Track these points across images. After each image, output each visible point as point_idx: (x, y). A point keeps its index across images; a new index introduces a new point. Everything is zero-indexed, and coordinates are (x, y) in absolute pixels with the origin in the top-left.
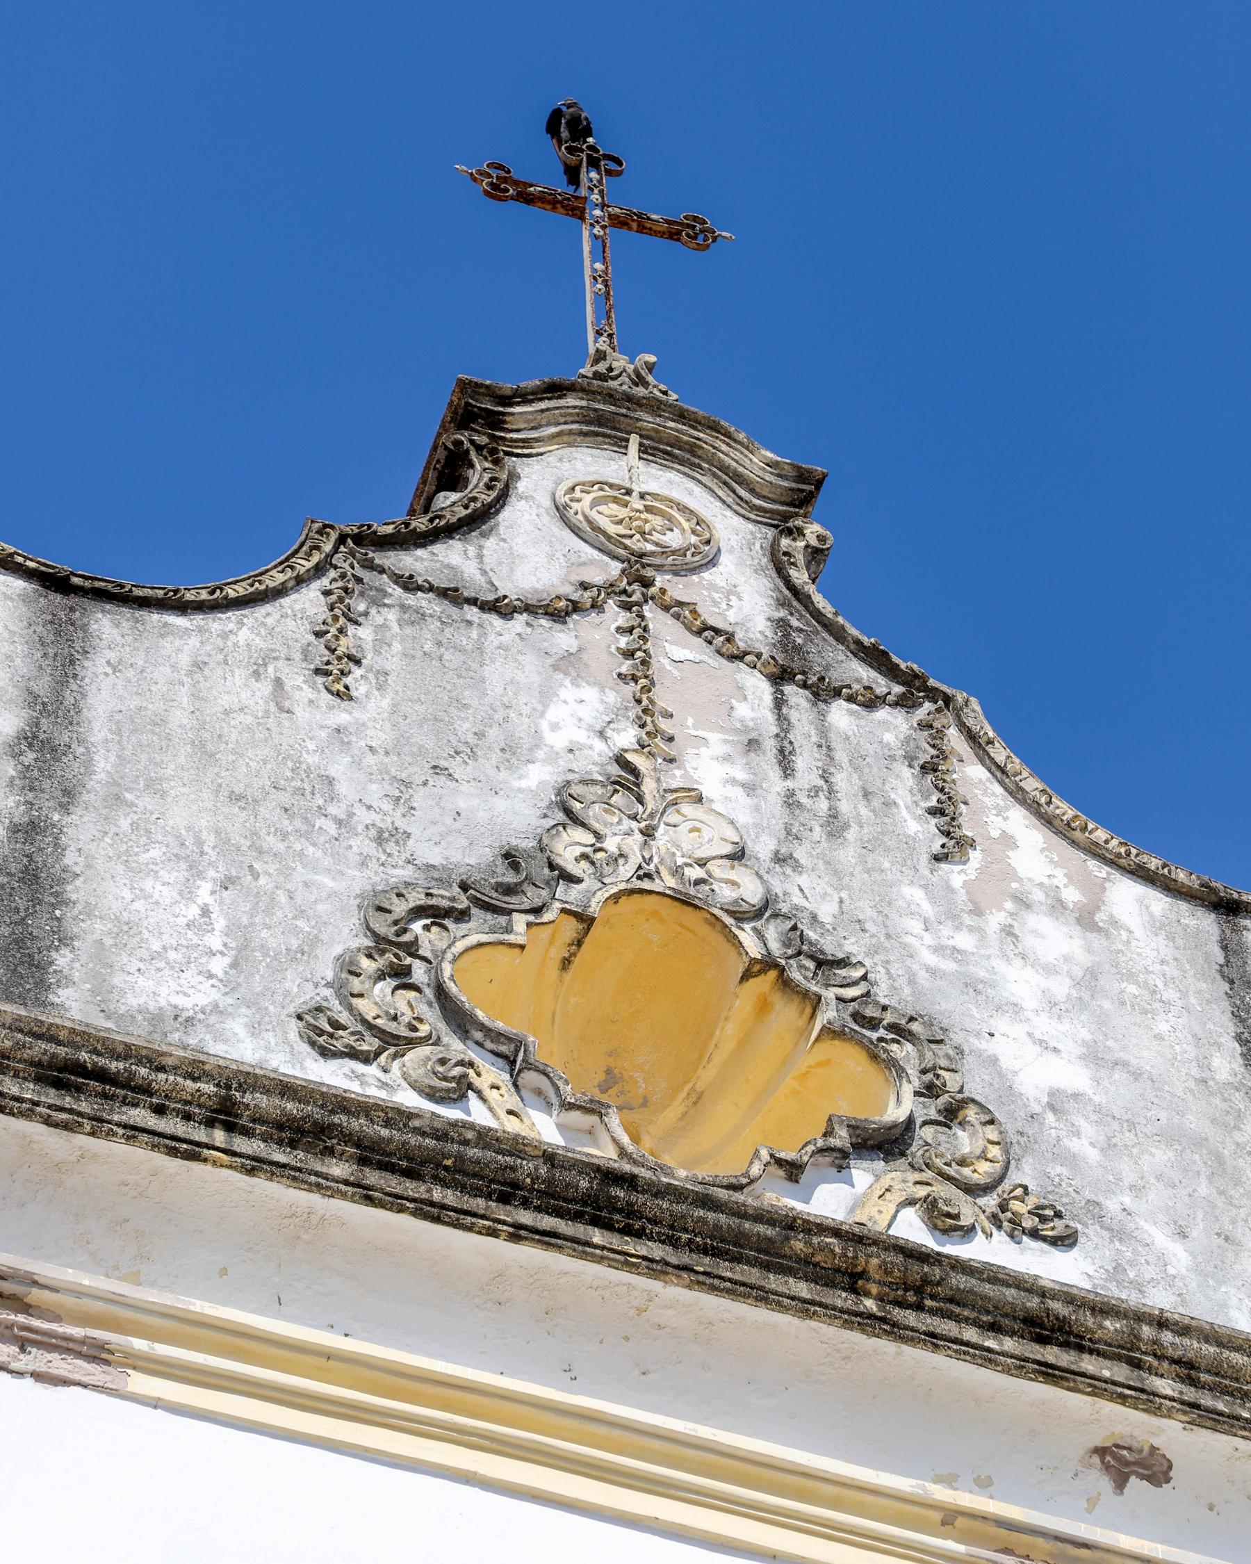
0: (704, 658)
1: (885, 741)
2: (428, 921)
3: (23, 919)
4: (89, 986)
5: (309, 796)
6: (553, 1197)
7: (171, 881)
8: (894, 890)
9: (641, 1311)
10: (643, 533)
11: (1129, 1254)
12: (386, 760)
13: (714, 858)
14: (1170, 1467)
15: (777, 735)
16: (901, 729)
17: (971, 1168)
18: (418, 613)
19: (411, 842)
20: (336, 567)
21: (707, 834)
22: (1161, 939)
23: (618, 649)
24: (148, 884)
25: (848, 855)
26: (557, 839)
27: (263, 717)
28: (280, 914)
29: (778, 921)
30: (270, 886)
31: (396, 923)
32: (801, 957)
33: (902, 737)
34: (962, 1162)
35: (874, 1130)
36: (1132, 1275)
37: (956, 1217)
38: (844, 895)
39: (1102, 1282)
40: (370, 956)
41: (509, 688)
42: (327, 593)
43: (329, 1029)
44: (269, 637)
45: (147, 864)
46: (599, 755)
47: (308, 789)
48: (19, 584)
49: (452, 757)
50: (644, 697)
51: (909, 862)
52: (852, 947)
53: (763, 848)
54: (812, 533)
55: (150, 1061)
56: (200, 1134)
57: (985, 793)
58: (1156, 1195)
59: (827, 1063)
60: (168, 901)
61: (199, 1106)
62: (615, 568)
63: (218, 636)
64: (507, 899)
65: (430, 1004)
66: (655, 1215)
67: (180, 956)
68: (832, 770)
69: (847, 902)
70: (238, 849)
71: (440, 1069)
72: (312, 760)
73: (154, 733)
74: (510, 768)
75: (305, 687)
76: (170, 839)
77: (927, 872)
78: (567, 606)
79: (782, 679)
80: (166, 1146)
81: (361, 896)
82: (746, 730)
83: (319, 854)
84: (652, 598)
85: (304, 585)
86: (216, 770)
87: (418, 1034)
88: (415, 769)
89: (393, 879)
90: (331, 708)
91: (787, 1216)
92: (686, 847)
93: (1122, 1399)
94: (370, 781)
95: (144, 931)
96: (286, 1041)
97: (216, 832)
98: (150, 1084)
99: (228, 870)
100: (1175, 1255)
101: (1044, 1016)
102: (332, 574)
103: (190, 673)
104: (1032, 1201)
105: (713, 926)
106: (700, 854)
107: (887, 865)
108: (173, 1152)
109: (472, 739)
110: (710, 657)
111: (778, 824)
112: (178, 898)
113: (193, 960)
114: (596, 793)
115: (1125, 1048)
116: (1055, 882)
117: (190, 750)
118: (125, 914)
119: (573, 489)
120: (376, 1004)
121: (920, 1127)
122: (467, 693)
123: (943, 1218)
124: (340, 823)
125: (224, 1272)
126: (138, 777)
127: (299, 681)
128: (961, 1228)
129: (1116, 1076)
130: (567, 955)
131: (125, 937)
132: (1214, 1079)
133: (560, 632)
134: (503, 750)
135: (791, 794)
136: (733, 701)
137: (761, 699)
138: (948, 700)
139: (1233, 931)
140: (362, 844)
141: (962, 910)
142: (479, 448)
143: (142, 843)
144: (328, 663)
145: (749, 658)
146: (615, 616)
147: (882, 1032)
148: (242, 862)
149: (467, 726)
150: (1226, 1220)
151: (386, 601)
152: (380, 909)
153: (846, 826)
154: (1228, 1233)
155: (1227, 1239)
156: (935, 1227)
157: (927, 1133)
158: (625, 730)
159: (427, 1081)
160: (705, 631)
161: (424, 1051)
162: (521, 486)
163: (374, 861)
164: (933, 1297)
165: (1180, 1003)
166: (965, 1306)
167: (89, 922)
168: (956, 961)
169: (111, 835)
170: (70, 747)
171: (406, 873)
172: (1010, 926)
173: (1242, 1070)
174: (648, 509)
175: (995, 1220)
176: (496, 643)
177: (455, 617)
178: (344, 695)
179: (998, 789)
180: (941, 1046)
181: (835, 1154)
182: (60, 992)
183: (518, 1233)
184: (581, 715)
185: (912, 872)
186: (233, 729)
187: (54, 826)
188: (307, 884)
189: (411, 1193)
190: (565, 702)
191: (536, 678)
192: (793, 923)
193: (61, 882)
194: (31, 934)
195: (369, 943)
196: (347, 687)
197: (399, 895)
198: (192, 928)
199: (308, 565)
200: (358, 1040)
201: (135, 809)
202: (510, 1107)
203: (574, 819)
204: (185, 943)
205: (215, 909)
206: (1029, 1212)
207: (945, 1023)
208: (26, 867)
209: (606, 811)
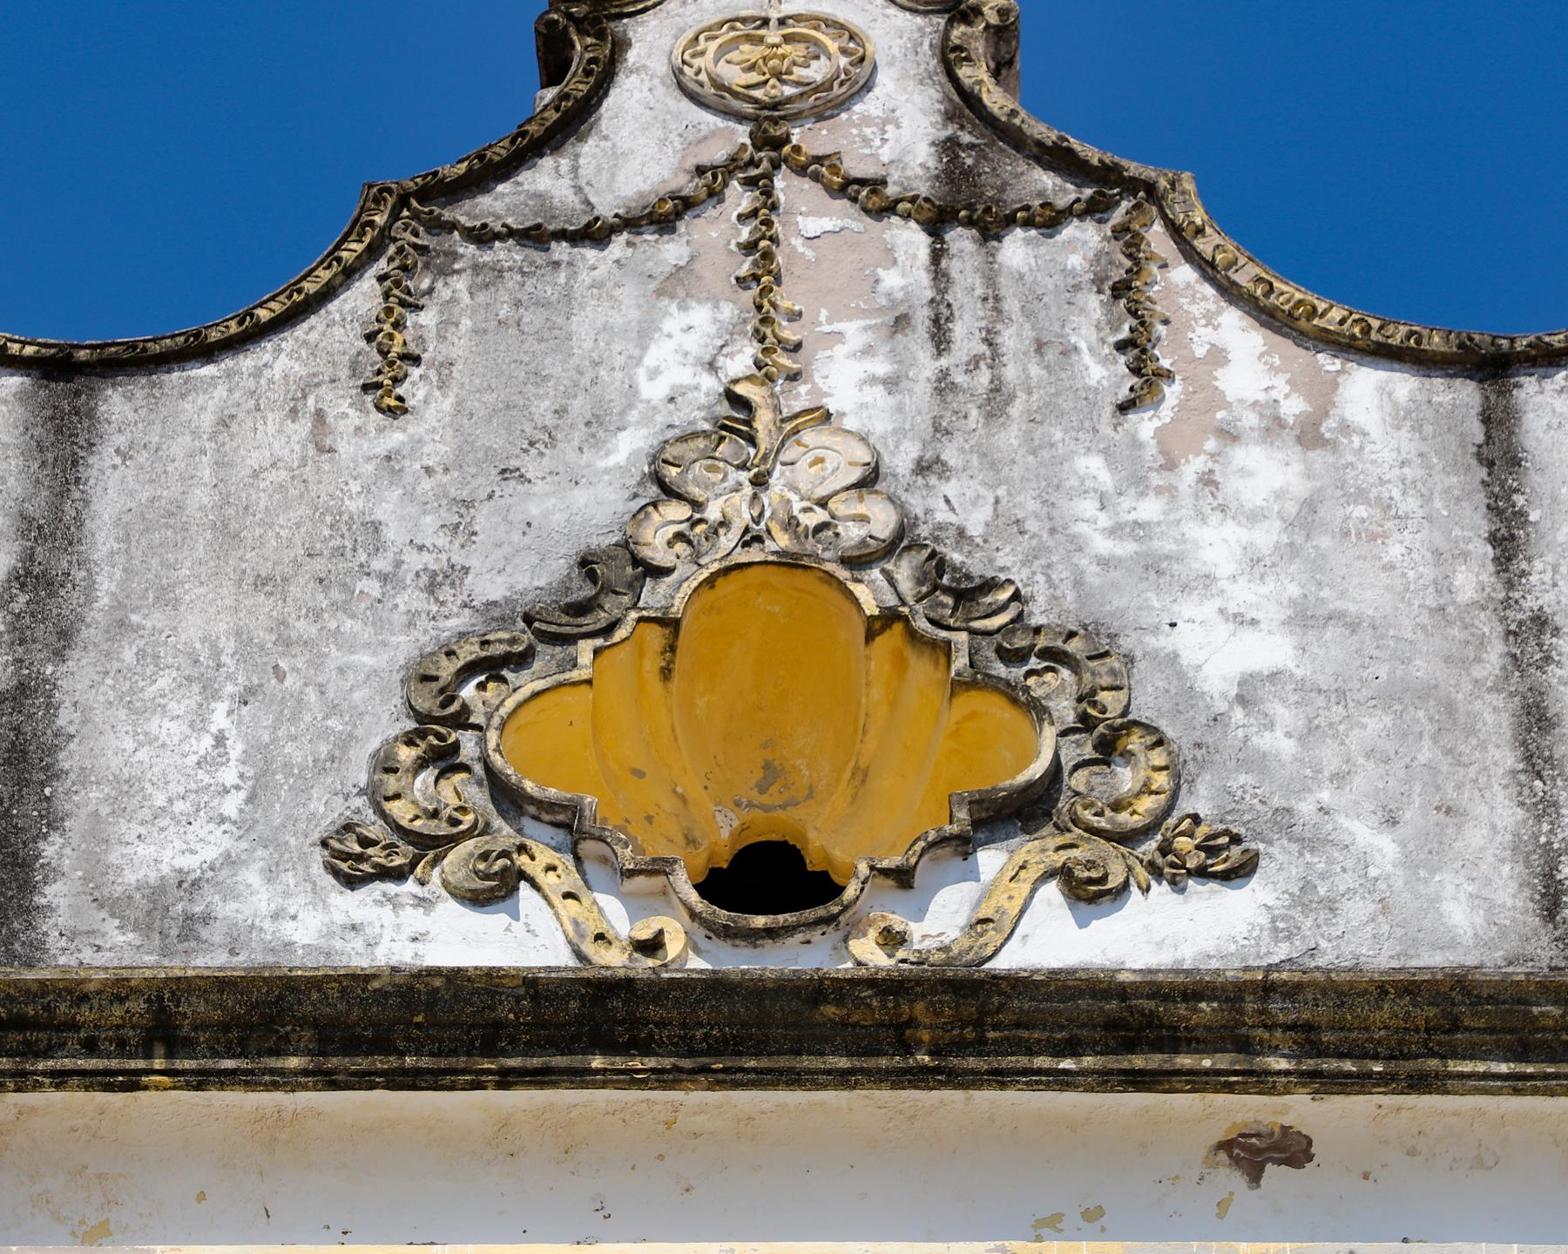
0: (848, 222)
1: (1069, 267)
2: (482, 678)
3: (7, 810)
4: (80, 873)
5: (349, 554)
6: (544, 1027)
7: (181, 713)
8: (1066, 466)
9: (669, 1124)
10: (778, 75)
11: (1322, 865)
12: (445, 479)
13: (837, 493)
14: (1310, 1143)
15: (932, 301)
16: (1091, 245)
17: (1130, 809)
18: (494, 270)
19: (469, 580)
20: (395, 240)
21: (832, 461)
22: (1404, 434)
23: (738, 244)
24: (154, 725)
25: (1009, 438)
26: (645, 524)
27: (299, 467)
28: (308, 718)
29: (913, 553)
30: (298, 684)
31: (442, 691)
32: (938, 593)
33: (1091, 255)
34: (1117, 806)
35: (1004, 798)
36: (1322, 891)
37: (1103, 880)
38: (1001, 492)
39: (1283, 911)
40: (410, 743)
41: (600, 338)
42: (381, 279)
43: (357, 849)
44: (312, 359)
45: (154, 698)
46: (707, 394)
47: (349, 544)
49: (525, 451)
50: (765, 303)
51: (1087, 424)
52: (1008, 561)
53: (901, 461)
54: (991, 8)
55: (70, 992)
56: (141, 1064)
57: (1193, 301)
58: (1366, 778)
59: (972, 716)
60: (176, 739)
61: (133, 1027)
62: (742, 134)
63: (250, 375)
64: (581, 620)
65: (480, 783)
66: (662, 1017)
67: (188, 804)
68: (999, 327)
69: (1004, 501)
70: (262, 648)
71: (481, 866)
72: (353, 506)
73: (167, 526)
74: (595, 446)
75: (351, 412)
76: (181, 658)
77: (1109, 431)
78: (675, 205)
79: (943, 222)
80: (100, 1084)
81: (406, 667)
82: (894, 303)
83: (358, 626)
84: (786, 161)
85: (357, 276)
86: (240, 553)
87: (462, 827)
88: (481, 480)
89: (446, 634)
90: (380, 430)
91: (812, 979)
92: (803, 487)
93: (1229, 1088)
94: (425, 512)
95: (148, 785)
96: (308, 879)
97: (237, 633)
98: (74, 1018)
99: (248, 679)
100: (1380, 850)
101: (1242, 581)
102: (392, 250)
103: (213, 437)
104: (1202, 832)
105: (827, 582)
106: (821, 492)
107: (1058, 435)
108: (109, 1088)
109: (550, 420)
110: (855, 219)
111: (923, 421)
112: (188, 731)
113: (202, 805)
114: (698, 448)
115: (1343, 595)
116: (1274, 394)
117: (208, 535)
118: (125, 770)
119: (696, 38)
120: (413, 802)
121: (1071, 774)
122: (548, 360)
123: (1084, 887)
124: (384, 578)
125: (201, 1197)
126: (147, 589)
127: (344, 405)
128: (1109, 892)
129: (1328, 635)
130: (663, 664)
131: (125, 799)
132: (1454, 603)
133: (668, 242)
134: (588, 424)
135: (944, 374)
136: (880, 271)
137: (915, 257)
138: (1150, 188)
139: (1500, 393)
140: (411, 599)
141: (1150, 468)
142: (578, 22)
143: (149, 674)
144: (379, 372)
145: (901, 207)
146: (739, 198)
147: (1034, 663)
148: (265, 664)
149: (547, 403)
150: (1449, 787)
151: (456, 266)
152: (426, 679)
153: (1012, 397)
154: (1451, 804)
155: (1448, 811)
156: (1079, 898)
157: (1079, 781)
158: (740, 351)
159: (467, 885)
160: (848, 188)
161: (468, 846)
162: (632, 56)
163: (424, 616)
164: (995, 1027)
165: (1421, 512)
166: (1034, 1027)
167: (83, 793)
168: (1137, 539)
169: (112, 674)
170: (69, 574)
171: (460, 621)
172: (1211, 471)
173: (1493, 580)
174: (788, 39)
175: (1155, 871)
176: (588, 281)
177: (539, 262)
178: (397, 411)
179: (1208, 290)
180: (1107, 660)
181: (954, 843)
182: (47, 890)
183: (506, 1080)
184: (686, 348)
185: (1089, 437)
186: (262, 494)
187: (46, 681)
188: (341, 671)
189: (379, 1066)
190: (669, 336)
191: (634, 314)
192: (929, 550)
193: (53, 750)
194: (15, 827)
195: (411, 725)
196: (400, 399)
197: (450, 654)
198: (203, 765)
199: (359, 247)
200: (389, 855)
201: (141, 632)
202: (566, 889)
203: (670, 492)
204: (193, 786)
205: (231, 733)
206: (1198, 847)
207: (1115, 627)
208: (13, 743)
209: (709, 469)
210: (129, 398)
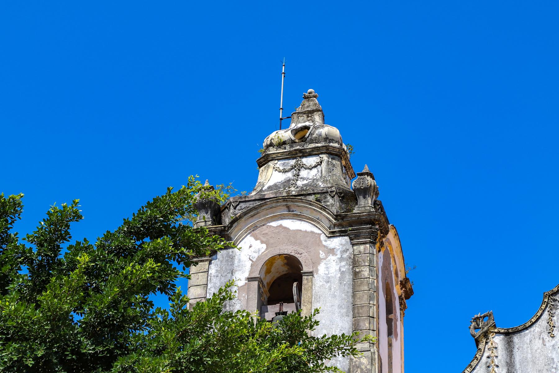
48: (502, 337)
72: (550, 355)
210: (517, 338)
